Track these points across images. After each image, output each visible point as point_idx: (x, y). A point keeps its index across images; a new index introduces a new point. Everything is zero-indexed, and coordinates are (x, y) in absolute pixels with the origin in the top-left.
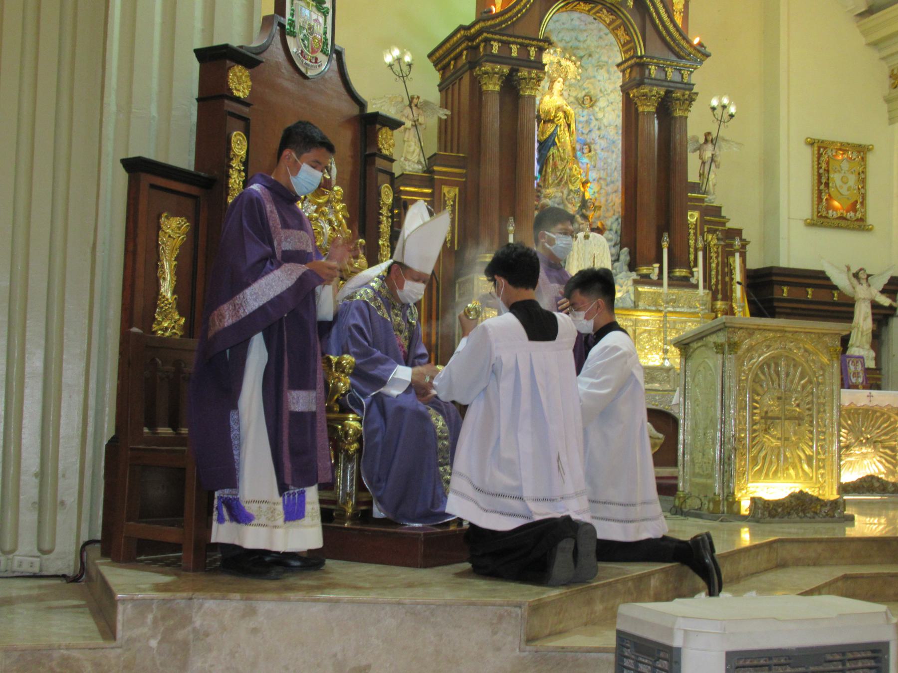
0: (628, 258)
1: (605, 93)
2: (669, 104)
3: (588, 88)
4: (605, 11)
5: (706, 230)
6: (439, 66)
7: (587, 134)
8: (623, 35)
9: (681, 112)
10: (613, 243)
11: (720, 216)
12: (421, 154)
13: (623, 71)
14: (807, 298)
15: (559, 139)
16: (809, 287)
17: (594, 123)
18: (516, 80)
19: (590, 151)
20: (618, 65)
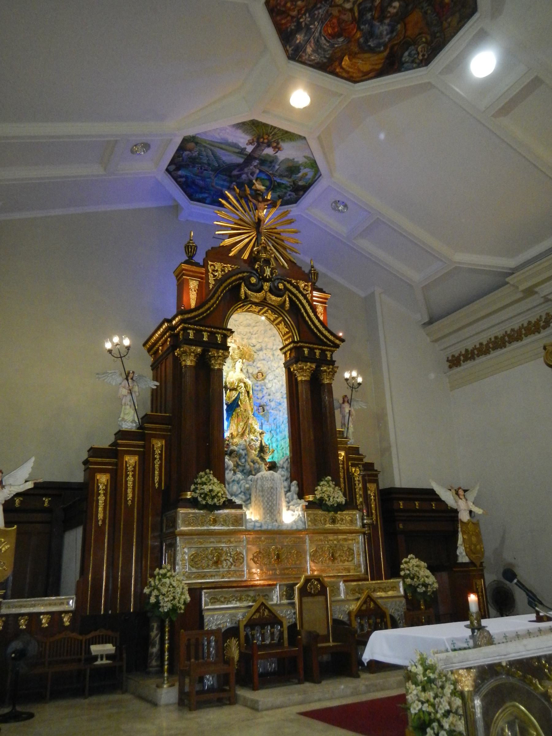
0: (297, 489)
1: (272, 370)
2: (319, 375)
3: (260, 367)
4: (270, 311)
5: (350, 465)
6: (152, 352)
7: (261, 399)
8: (283, 328)
9: (327, 380)
10: (285, 478)
11: (358, 454)
12: (136, 415)
13: (285, 353)
14: (416, 508)
15: (241, 401)
16: (416, 501)
17: (265, 391)
18: (207, 358)
19: (264, 411)
20: (281, 349)
